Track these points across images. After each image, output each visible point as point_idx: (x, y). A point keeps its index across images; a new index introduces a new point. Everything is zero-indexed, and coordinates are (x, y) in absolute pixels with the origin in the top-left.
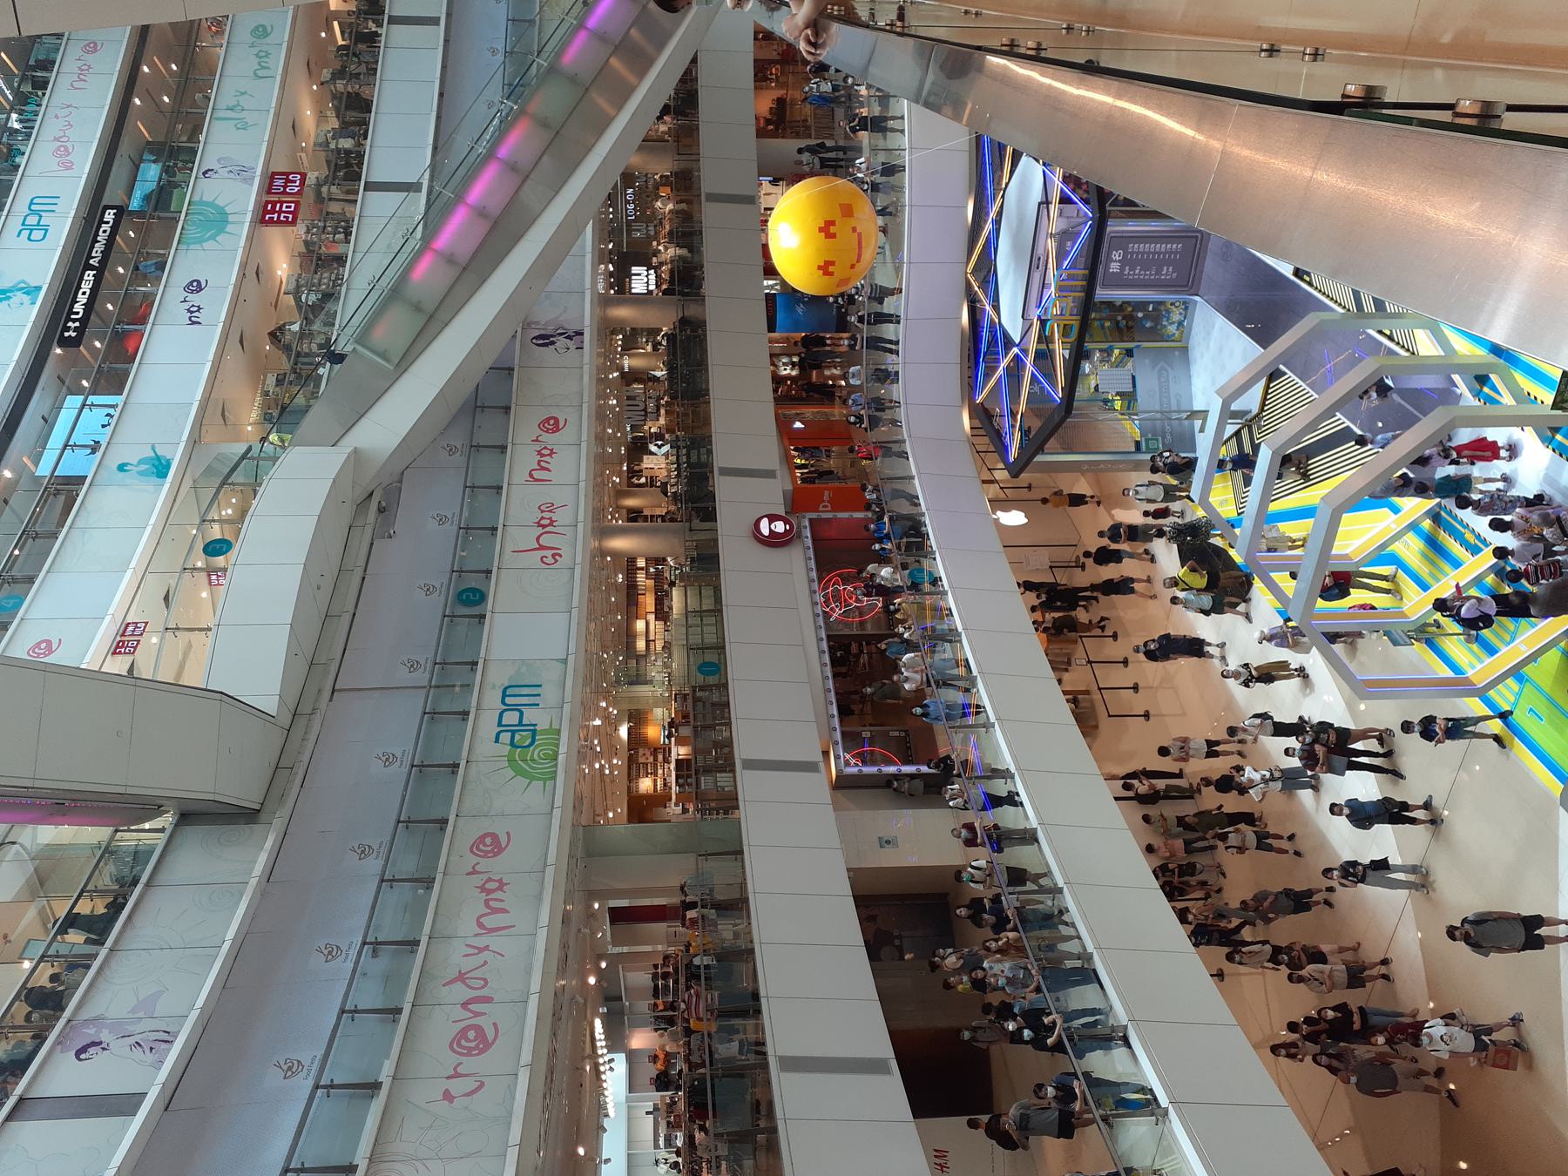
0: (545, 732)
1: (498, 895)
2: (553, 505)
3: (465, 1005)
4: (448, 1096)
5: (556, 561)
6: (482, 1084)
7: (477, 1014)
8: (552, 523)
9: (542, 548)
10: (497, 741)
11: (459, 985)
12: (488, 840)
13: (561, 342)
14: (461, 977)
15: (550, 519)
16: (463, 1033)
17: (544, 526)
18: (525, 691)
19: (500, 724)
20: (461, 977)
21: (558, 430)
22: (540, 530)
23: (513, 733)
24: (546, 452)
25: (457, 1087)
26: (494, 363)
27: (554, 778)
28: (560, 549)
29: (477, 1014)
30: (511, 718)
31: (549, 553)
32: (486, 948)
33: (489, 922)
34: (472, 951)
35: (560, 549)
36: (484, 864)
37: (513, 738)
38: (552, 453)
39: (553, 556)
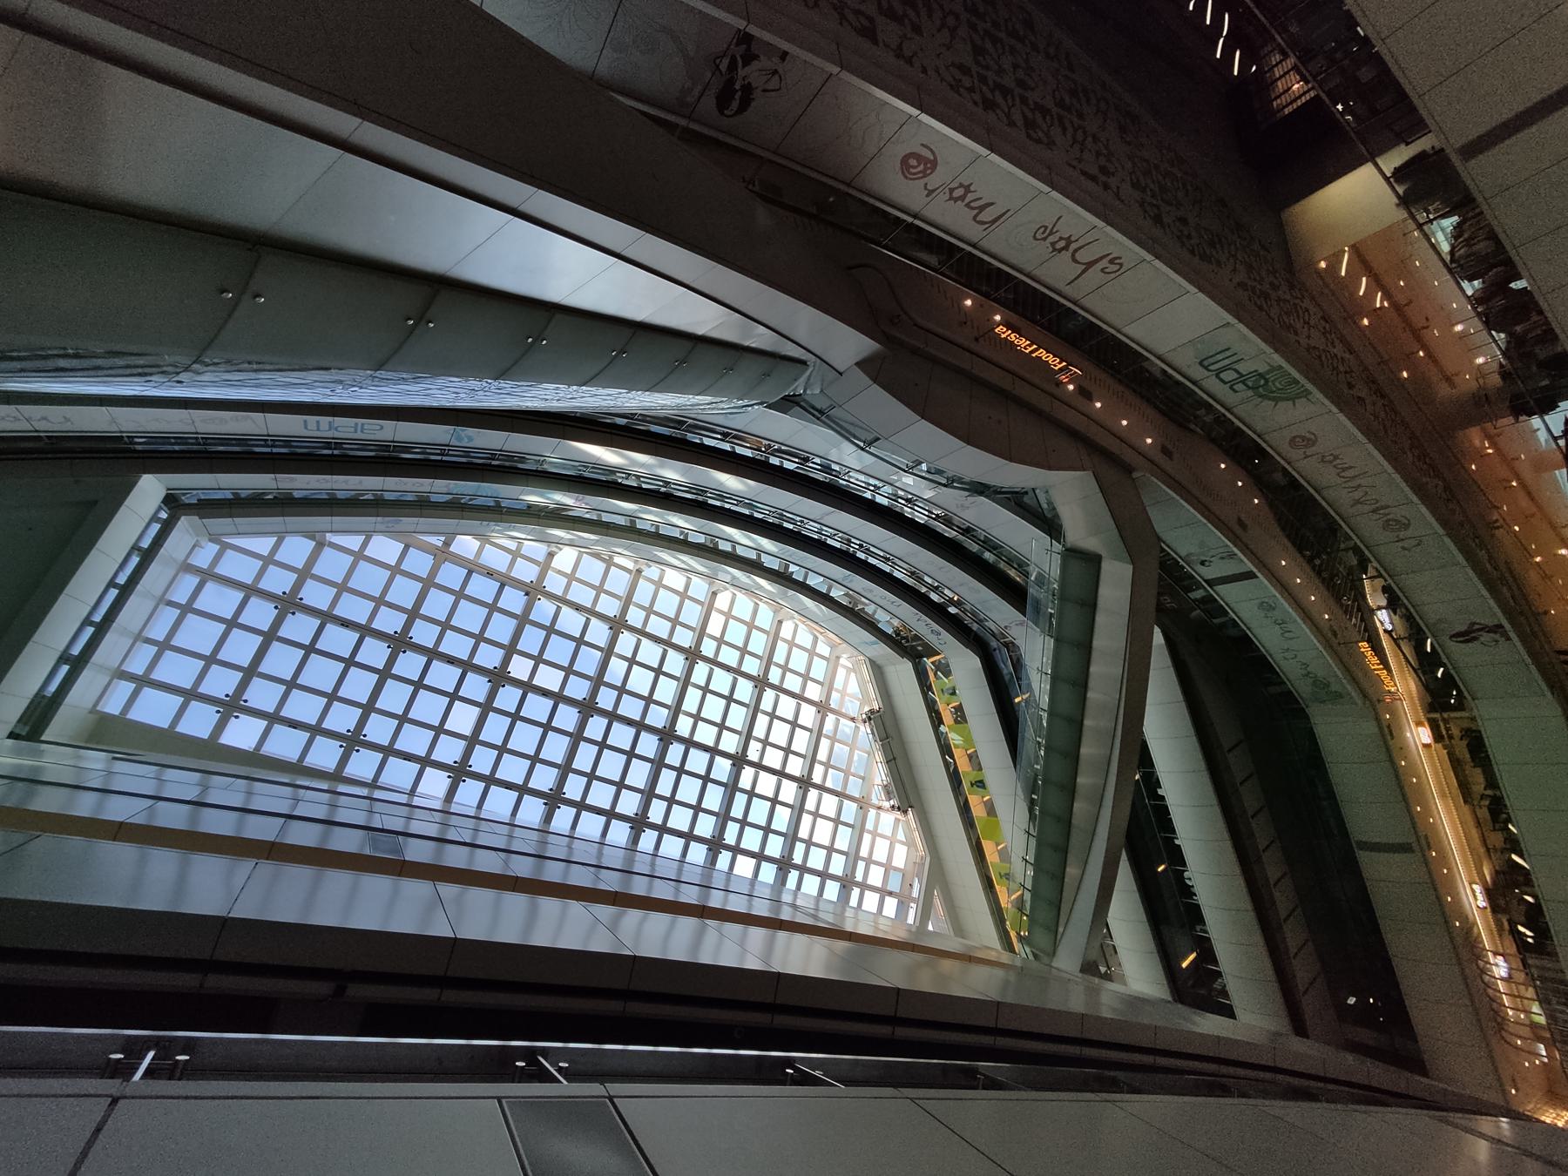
0: (1268, 372)
1: (1338, 461)
2: (1046, 227)
3: (1374, 511)
5: (1121, 265)
8: (1069, 241)
9: (1090, 265)
10: (1236, 392)
13: (752, 73)
14: (1358, 502)
17: (1066, 248)
18: (1219, 357)
19: (1225, 383)
20: (1358, 502)
21: (934, 164)
22: (1067, 255)
23: (1243, 382)
24: (959, 192)
25: (1406, 544)
26: (1127, 563)
28: (1111, 254)
30: (1229, 376)
31: (1104, 263)
32: (1359, 486)
33: (1347, 474)
34: (1350, 490)
35: (1111, 254)
37: (1247, 386)
38: (967, 189)
39: (1111, 262)
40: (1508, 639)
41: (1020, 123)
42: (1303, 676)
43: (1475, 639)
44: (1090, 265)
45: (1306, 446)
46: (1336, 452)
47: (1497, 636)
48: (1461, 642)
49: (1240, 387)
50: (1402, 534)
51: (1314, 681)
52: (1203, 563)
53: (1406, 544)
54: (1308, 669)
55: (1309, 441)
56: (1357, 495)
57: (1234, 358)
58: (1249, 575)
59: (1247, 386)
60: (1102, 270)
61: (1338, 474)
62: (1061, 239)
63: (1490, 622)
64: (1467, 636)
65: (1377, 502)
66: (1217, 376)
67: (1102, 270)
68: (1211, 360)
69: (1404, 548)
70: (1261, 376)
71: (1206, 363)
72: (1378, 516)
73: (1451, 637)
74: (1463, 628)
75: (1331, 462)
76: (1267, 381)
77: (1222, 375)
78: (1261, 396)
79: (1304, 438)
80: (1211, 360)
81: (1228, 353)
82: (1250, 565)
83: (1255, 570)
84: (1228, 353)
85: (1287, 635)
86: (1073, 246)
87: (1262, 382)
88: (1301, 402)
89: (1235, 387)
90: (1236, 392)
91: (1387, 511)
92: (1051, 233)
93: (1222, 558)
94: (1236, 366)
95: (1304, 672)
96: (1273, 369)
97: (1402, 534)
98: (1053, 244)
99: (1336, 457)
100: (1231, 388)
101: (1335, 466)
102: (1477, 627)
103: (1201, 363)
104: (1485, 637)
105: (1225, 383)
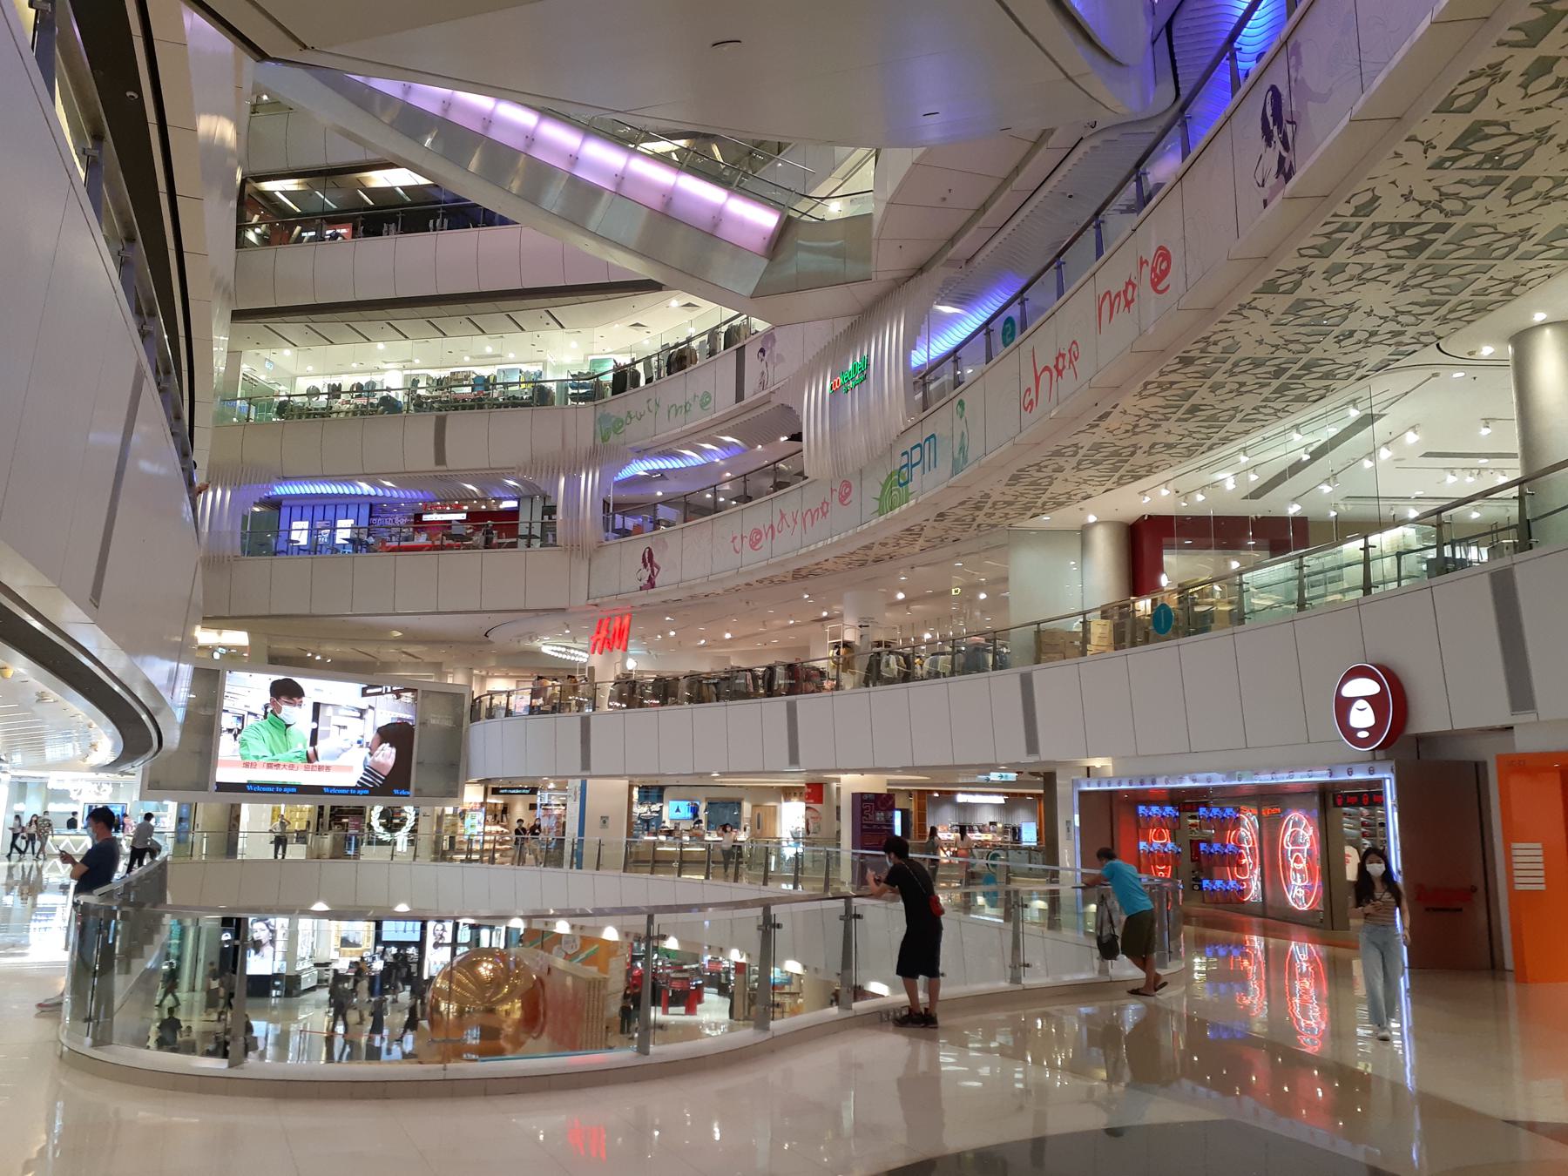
0: (907, 490)
1: (821, 514)
3: (772, 527)
4: (734, 538)
5: (1026, 409)
6: (737, 552)
7: (766, 535)
8: (1060, 373)
9: (1037, 379)
10: (903, 454)
11: (779, 517)
12: (848, 489)
14: (783, 516)
15: (1064, 367)
16: (759, 532)
17: (1056, 367)
19: (912, 449)
20: (783, 516)
23: (906, 465)
25: (738, 540)
27: (880, 515)
29: (766, 535)
32: (796, 523)
36: (836, 494)
39: (1031, 403)
40: (641, 589)
41: (1161, 379)
42: (629, 413)
43: (645, 566)
44: (1037, 379)
45: (841, 493)
46: (828, 515)
47: (645, 581)
48: (644, 555)
49: (905, 460)
50: (746, 541)
51: (622, 421)
52: (762, 351)
53: (738, 540)
54: (635, 419)
55: (842, 499)
56: (789, 519)
57: (927, 466)
58: (740, 396)
59: (902, 468)
60: (1029, 390)
61: (810, 510)
62: (1064, 367)
63: (657, 581)
64: (648, 560)
65: (780, 532)
66: (919, 445)
67: (1029, 390)
68: (932, 446)
69: (734, 538)
70: (907, 482)
71: (932, 440)
72: (767, 528)
73: (650, 550)
74: (656, 559)
75: (822, 508)
76: (901, 485)
77: (919, 449)
78: (891, 476)
79: (848, 494)
80: (932, 446)
81: (932, 464)
82: (750, 400)
83: (743, 403)
84: (932, 464)
85: (673, 409)
86: (1055, 374)
87: (901, 481)
88: (875, 505)
89: (906, 456)
90: (903, 454)
91: (770, 534)
92: (1071, 361)
93: (763, 373)
94: (920, 466)
95: (633, 414)
96: (908, 494)
97: (746, 541)
98: (1063, 356)
99: (824, 514)
100: (906, 453)
101: (817, 510)
102: (656, 570)
103: (933, 436)
104: (646, 574)
105: (912, 449)
